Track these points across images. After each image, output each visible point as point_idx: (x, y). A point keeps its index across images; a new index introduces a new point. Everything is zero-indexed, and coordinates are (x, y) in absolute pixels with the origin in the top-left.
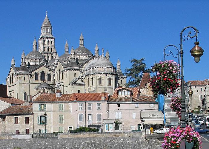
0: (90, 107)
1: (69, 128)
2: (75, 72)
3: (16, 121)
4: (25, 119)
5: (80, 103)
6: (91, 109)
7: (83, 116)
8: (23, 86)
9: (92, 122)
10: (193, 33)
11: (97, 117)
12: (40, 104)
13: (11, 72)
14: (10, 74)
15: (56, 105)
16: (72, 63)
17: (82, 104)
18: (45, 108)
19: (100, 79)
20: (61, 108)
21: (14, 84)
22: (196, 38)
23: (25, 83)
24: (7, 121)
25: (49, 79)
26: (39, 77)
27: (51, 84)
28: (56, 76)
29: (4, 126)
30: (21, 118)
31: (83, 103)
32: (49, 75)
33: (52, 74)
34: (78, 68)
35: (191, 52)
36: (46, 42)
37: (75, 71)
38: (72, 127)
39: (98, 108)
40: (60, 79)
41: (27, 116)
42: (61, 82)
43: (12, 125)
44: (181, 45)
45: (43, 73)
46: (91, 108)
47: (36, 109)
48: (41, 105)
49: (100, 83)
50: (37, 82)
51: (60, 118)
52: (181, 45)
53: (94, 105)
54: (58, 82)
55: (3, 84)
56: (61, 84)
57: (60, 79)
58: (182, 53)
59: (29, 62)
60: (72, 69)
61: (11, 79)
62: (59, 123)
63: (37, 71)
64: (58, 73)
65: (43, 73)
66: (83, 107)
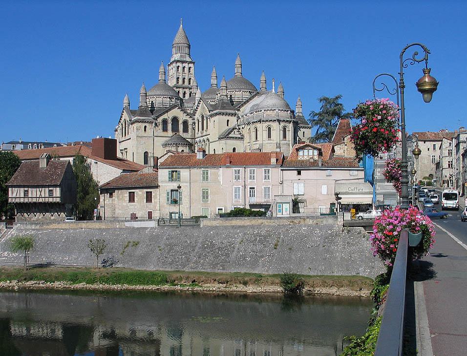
0: (252, 175)
1: (219, 209)
2: (227, 118)
3: (132, 198)
4: (145, 195)
5: (236, 169)
6: (254, 179)
7: (241, 190)
8: (143, 141)
9: (255, 200)
10: (421, 55)
11: (263, 191)
12: (170, 170)
13: (123, 119)
14: (122, 121)
15: (197, 172)
16: (223, 103)
17: (239, 171)
18: (179, 178)
19: (269, 129)
20: (205, 178)
21: (127, 137)
22: (426, 63)
23: (145, 135)
24: (116, 199)
25: (186, 130)
26: (170, 126)
27: (190, 137)
28: (197, 124)
29: (112, 206)
30: (140, 194)
31: (242, 169)
32: (185, 123)
33: (190, 121)
34: (233, 112)
35: (418, 85)
36: (180, 69)
37: (227, 117)
38: (223, 208)
39: (266, 177)
40: (203, 129)
41: (149, 190)
42: (204, 134)
43: (125, 204)
44: (401, 74)
45: (175, 120)
46: (254, 177)
47: (163, 179)
48: (173, 172)
49: (269, 136)
50: (165, 134)
51: (204, 192)
52: (401, 74)
53: (260, 171)
54: (200, 135)
55: (110, 138)
56: (205, 138)
57: (203, 129)
58: (403, 87)
59: (152, 102)
60: (223, 114)
61: (124, 129)
62: (201, 202)
63: (165, 116)
64: (200, 120)
65: (175, 120)
66: (242, 174)
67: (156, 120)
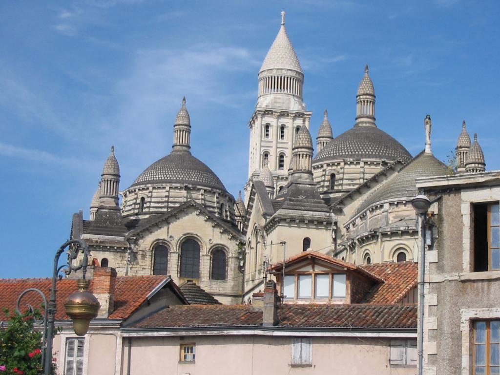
16: (297, 192)
25: (218, 273)
27: (229, 292)
32: (218, 253)
33: (232, 247)
34: (322, 215)
45: (190, 244)
59: (143, 199)
60: (311, 222)
63: (160, 234)
65: (190, 244)
67: (136, 242)
